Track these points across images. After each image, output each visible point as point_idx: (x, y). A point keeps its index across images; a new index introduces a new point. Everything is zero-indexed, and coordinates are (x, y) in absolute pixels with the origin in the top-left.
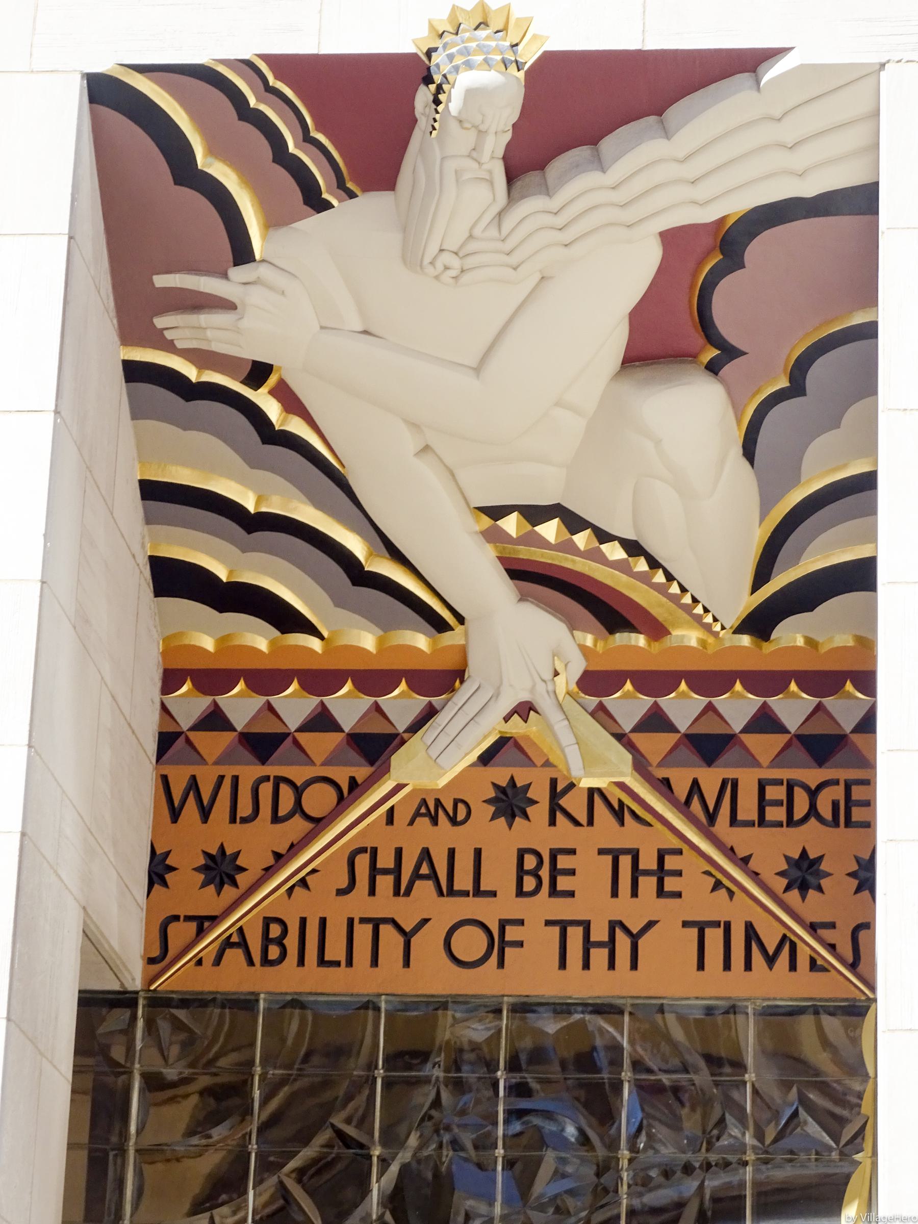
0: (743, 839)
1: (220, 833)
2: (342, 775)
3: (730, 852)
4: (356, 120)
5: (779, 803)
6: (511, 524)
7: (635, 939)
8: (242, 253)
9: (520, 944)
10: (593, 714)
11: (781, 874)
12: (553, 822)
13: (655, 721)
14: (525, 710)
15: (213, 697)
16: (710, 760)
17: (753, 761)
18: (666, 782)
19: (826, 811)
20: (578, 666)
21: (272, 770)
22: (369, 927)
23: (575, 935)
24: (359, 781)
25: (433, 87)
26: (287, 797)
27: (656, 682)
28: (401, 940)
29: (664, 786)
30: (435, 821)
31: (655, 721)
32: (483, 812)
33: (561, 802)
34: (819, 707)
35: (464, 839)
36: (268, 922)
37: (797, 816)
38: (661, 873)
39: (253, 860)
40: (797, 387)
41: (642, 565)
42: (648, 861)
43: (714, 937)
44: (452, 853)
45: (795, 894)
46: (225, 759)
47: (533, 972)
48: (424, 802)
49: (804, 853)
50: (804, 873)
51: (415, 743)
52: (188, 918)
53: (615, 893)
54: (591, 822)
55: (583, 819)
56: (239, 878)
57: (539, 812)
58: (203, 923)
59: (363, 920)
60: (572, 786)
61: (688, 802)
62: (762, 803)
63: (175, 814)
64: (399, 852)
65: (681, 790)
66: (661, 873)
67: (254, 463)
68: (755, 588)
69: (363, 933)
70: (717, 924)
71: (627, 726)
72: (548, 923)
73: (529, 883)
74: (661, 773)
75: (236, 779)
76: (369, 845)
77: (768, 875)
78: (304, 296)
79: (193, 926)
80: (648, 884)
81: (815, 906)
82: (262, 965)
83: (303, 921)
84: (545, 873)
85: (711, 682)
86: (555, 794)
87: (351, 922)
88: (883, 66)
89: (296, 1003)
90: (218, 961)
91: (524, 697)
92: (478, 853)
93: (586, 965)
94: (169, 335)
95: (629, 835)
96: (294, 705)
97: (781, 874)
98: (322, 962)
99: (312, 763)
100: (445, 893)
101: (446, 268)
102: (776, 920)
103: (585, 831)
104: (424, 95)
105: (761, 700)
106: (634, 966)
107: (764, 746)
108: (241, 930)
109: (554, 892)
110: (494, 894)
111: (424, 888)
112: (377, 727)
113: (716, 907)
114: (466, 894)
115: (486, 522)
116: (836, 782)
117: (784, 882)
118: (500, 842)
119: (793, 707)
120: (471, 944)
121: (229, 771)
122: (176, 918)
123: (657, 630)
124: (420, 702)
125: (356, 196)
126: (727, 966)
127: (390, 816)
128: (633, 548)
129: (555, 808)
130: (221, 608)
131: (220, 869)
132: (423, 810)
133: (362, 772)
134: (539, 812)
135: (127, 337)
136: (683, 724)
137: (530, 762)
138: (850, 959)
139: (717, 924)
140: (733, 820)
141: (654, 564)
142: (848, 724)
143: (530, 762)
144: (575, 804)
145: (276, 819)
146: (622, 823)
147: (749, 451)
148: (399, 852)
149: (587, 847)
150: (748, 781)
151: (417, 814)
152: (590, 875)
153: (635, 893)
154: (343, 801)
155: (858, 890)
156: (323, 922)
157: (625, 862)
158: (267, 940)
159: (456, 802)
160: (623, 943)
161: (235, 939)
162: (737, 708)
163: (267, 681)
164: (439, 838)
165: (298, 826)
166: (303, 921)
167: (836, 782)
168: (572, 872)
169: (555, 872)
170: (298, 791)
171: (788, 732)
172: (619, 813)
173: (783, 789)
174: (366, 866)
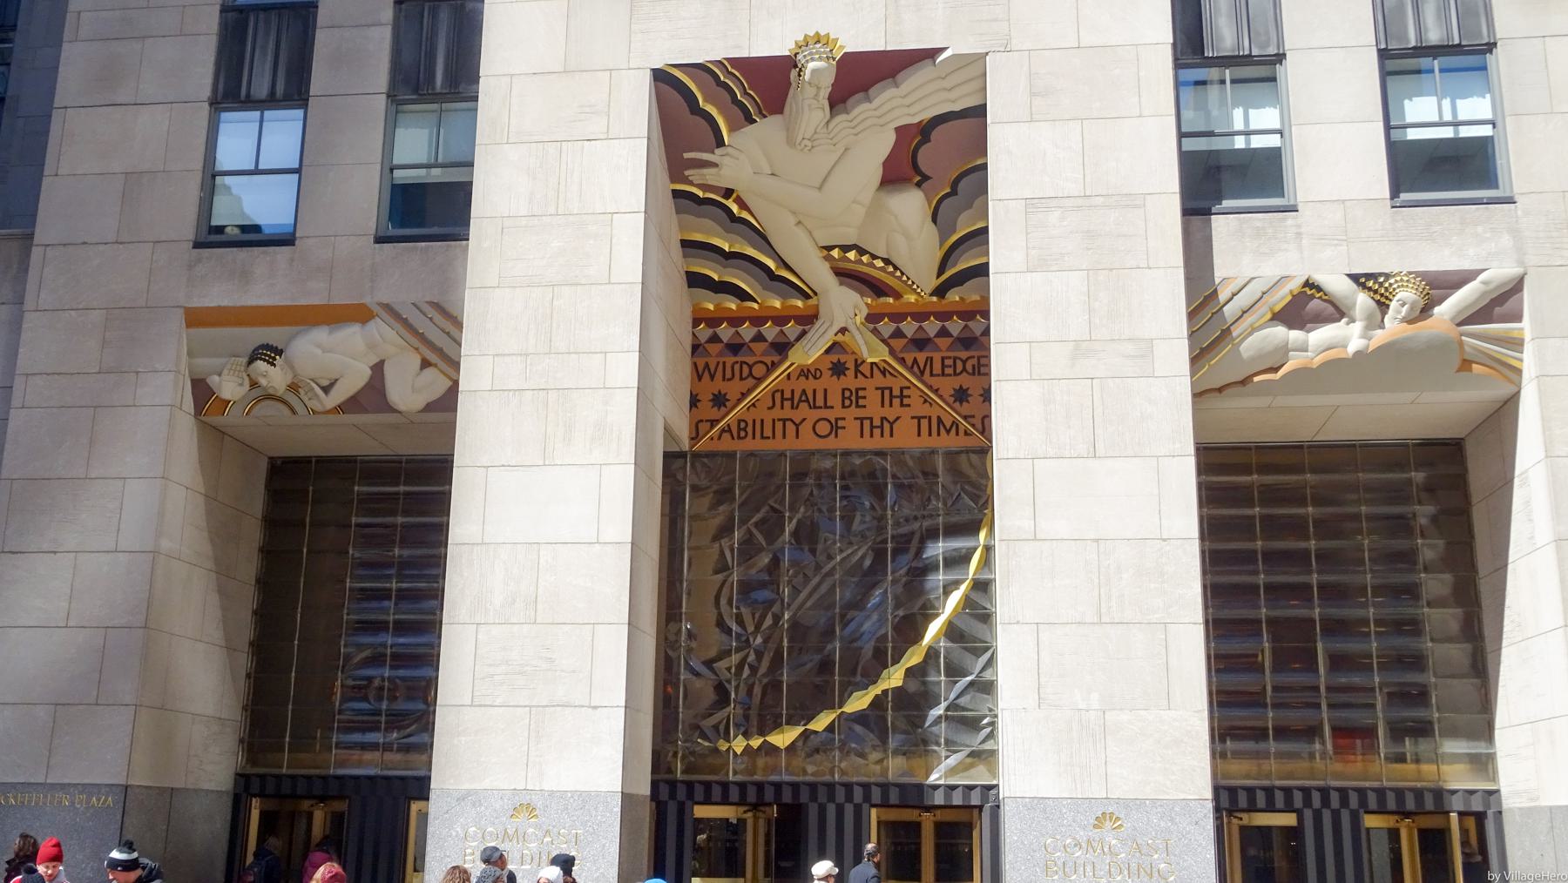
0: (933, 381)
1: (719, 385)
2: (768, 360)
3: (930, 387)
4: (765, 84)
6: (835, 253)
7: (891, 424)
8: (720, 143)
13: (898, 334)
14: (843, 330)
16: (921, 350)
17: (938, 349)
19: (969, 368)
20: (865, 311)
23: (867, 423)
26: (746, 370)
27: (897, 317)
29: (902, 361)
31: (898, 334)
35: (819, 385)
38: (902, 397)
39: (732, 396)
40: (954, 192)
41: (891, 269)
42: (896, 392)
43: (924, 423)
46: (720, 354)
47: (850, 439)
50: (961, 395)
51: (798, 345)
57: (850, 373)
58: (713, 423)
65: (909, 362)
66: (902, 397)
67: (727, 231)
68: (939, 276)
69: (779, 425)
71: (886, 336)
73: (847, 402)
77: (946, 396)
78: (746, 159)
80: (896, 402)
81: (966, 408)
85: (920, 316)
86: (857, 365)
89: (752, 454)
96: (747, 331)
102: (951, 414)
104: (794, 73)
107: (944, 342)
109: (858, 406)
111: (804, 406)
113: (925, 410)
118: (835, 386)
119: (955, 326)
120: (823, 428)
121: (722, 360)
123: (897, 295)
128: (887, 261)
129: (857, 371)
131: (719, 400)
133: (776, 359)
134: (850, 373)
135: (673, 180)
141: (896, 268)
142: (978, 333)
144: (865, 369)
145: (742, 379)
147: (934, 220)
149: (871, 386)
150: (937, 357)
152: (872, 398)
154: (769, 371)
157: (887, 393)
158: (739, 429)
160: (887, 426)
162: (931, 327)
163: (735, 321)
164: (809, 385)
165: (751, 381)
169: (858, 398)
170: (750, 367)
172: (884, 372)
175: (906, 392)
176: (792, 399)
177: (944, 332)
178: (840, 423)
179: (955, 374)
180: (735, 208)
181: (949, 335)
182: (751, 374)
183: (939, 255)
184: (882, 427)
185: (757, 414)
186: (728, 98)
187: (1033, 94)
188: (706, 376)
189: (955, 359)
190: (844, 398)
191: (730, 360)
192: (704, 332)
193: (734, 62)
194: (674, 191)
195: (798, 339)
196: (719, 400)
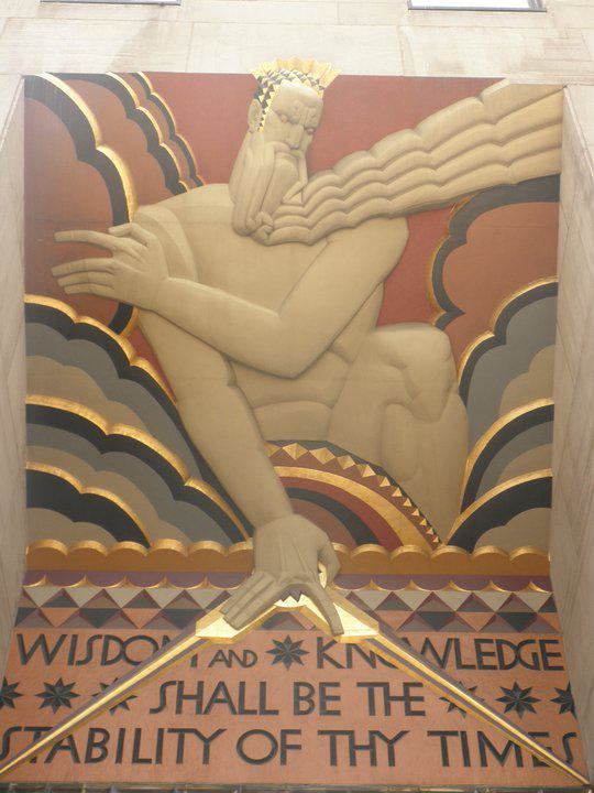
2: (157, 635)
3: (459, 684)
5: (492, 654)
7: (391, 743)
8: (120, 216)
9: (298, 747)
11: (501, 700)
12: (320, 665)
13: (392, 603)
15: (60, 588)
16: (437, 627)
17: (467, 628)
18: (405, 640)
21: (103, 631)
22: (176, 735)
23: (343, 742)
24: (171, 639)
25: (261, 98)
26: (114, 649)
28: (202, 744)
29: (405, 643)
30: (229, 666)
32: (266, 660)
33: (328, 652)
34: (511, 598)
35: (252, 677)
36: (93, 731)
40: (499, 339)
41: (386, 483)
42: (397, 689)
43: (454, 744)
44: (242, 684)
45: (513, 713)
49: (516, 686)
52: (28, 729)
53: (372, 711)
54: (350, 665)
55: (343, 662)
56: (73, 701)
57: (310, 659)
58: (39, 732)
59: (171, 731)
60: (334, 642)
62: (480, 654)
63: (26, 658)
64: (201, 684)
66: (407, 699)
67: (111, 395)
69: (171, 742)
70: (454, 733)
71: (373, 606)
72: (321, 732)
73: (304, 706)
74: (401, 635)
75: (75, 637)
76: (178, 678)
79: (32, 734)
82: (86, 762)
83: (122, 731)
84: (316, 698)
86: (322, 649)
87: (161, 731)
90: (49, 760)
91: (296, 582)
92: (263, 685)
93: (353, 762)
94: (62, 282)
95: (380, 673)
97: (501, 700)
98: (136, 759)
100: (237, 710)
101: (263, 223)
103: (346, 672)
105: (470, 592)
106: (392, 761)
107: (476, 619)
108: (71, 737)
109: (325, 712)
110: (275, 712)
111: (221, 710)
112: (184, 605)
114: (254, 712)
115: (275, 449)
116: (533, 641)
117: (504, 705)
118: (281, 681)
119: (495, 597)
120: (258, 747)
122: (19, 729)
125: (202, 185)
126: (467, 763)
127: (195, 658)
130: (76, 518)
133: (173, 633)
134: (310, 659)
135: (31, 288)
136: (414, 606)
138: (565, 757)
139: (454, 733)
140: (460, 666)
144: (337, 653)
145: (105, 662)
146: (374, 666)
147: (464, 393)
148: (201, 684)
150: (467, 640)
153: (388, 712)
154: (157, 651)
155: (563, 710)
156: (138, 731)
157: (379, 692)
158: (91, 744)
159: (246, 652)
161: (66, 743)
162: (454, 597)
163: (101, 570)
164: (232, 676)
166: (122, 731)
167: (533, 641)
168: (337, 698)
169: (324, 698)
170: (124, 644)
171: (490, 610)
172: (371, 659)
173: (494, 645)
174: (172, 691)
175: (414, 692)
176: (199, 697)
177: (472, 604)
178: (291, 740)
180: (128, 350)
181: (483, 607)
182: (123, 654)
183: (470, 465)
184: (371, 747)
185: (125, 719)
186: (141, 140)
188: (38, 657)
189: (500, 643)
190: (298, 698)
191: (86, 633)
192: (41, 592)
193: (163, 80)
195: (213, 606)
196: (59, 696)
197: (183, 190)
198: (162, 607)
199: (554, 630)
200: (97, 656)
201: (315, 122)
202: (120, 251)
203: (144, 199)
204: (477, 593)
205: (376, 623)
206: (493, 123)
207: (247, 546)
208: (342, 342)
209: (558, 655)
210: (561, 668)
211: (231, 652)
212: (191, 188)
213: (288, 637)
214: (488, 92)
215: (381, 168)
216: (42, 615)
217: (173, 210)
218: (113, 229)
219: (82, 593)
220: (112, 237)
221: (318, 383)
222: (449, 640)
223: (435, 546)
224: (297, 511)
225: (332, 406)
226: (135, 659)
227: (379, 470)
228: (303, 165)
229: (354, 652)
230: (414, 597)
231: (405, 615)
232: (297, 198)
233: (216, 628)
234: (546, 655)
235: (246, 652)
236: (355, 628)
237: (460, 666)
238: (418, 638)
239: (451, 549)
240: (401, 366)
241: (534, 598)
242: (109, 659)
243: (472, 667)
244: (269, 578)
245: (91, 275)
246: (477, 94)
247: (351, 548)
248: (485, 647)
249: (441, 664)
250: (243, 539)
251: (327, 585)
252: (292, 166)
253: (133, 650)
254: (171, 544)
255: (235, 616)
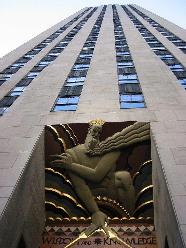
2: (71, 238)
5: (141, 241)
10: (111, 229)
12: (105, 244)
13: (120, 230)
15: (52, 228)
17: (136, 235)
26: (62, 241)
30: (85, 244)
32: (93, 243)
33: (106, 241)
34: (146, 228)
37: (145, 243)
48: (84, 241)
54: (111, 244)
55: (110, 243)
61: (127, 241)
62: (139, 241)
63: (44, 243)
75: (54, 238)
86: (105, 241)
88: (150, 122)
99: (67, 236)
107: (138, 233)
112: (77, 231)
115: (95, 198)
116: (150, 238)
121: (53, 237)
124: (84, 228)
130: (55, 213)
132: (84, 242)
133: (74, 237)
134: (102, 243)
137: (101, 236)
140: (134, 244)
143: (101, 236)
144: (108, 241)
145: (60, 244)
146: (116, 244)
147: (134, 185)
150: (136, 238)
151: (83, 243)
154: (71, 241)
159: (89, 241)
167: (150, 238)
170: (64, 240)
172: (115, 243)
177: (138, 230)
179: (144, 244)
181: (140, 231)
182: (63, 242)
187: (166, 128)
189: (143, 238)
191: (56, 237)
192: (48, 228)
193: (71, 125)
194: (46, 170)
195: (82, 231)
197: (75, 146)
198: (72, 231)
199: (154, 235)
200: (58, 242)
201: (101, 131)
202: (63, 158)
203: (68, 148)
204: (138, 227)
205: (117, 234)
206: (136, 130)
207: (90, 218)
208: (108, 175)
209: (156, 241)
210: (156, 244)
211: (86, 241)
212: (77, 145)
213: (98, 238)
214: (134, 124)
215: (114, 140)
216: (48, 233)
217: (73, 150)
218: (61, 154)
219: (56, 229)
220: (62, 156)
221: (104, 184)
222: (132, 238)
223: (130, 218)
224: (100, 210)
225: (107, 188)
226: (66, 243)
227: (117, 201)
228: (99, 140)
229: (112, 240)
230: (125, 228)
231: (123, 233)
232: (98, 147)
233: (83, 236)
234: (153, 241)
235: (89, 241)
236: (112, 235)
237: (134, 244)
238: (125, 238)
239: (133, 218)
240: (120, 179)
241: (151, 228)
242: (61, 243)
243: (137, 244)
244: (94, 225)
245: (57, 163)
246: (133, 124)
247: (112, 218)
248: (140, 240)
249: (131, 243)
250: (90, 217)
251: (107, 226)
252: (96, 140)
253: (65, 241)
254: (75, 218)
255: (87, 234)
